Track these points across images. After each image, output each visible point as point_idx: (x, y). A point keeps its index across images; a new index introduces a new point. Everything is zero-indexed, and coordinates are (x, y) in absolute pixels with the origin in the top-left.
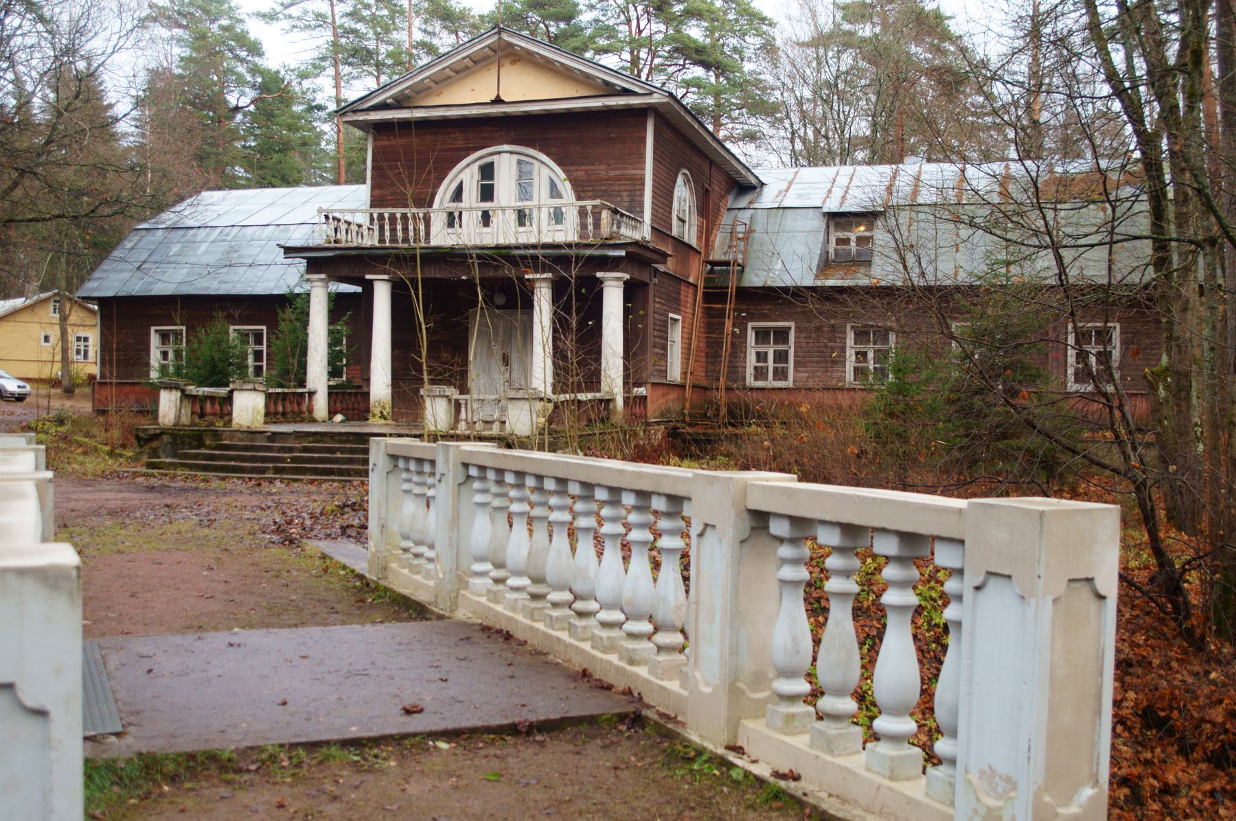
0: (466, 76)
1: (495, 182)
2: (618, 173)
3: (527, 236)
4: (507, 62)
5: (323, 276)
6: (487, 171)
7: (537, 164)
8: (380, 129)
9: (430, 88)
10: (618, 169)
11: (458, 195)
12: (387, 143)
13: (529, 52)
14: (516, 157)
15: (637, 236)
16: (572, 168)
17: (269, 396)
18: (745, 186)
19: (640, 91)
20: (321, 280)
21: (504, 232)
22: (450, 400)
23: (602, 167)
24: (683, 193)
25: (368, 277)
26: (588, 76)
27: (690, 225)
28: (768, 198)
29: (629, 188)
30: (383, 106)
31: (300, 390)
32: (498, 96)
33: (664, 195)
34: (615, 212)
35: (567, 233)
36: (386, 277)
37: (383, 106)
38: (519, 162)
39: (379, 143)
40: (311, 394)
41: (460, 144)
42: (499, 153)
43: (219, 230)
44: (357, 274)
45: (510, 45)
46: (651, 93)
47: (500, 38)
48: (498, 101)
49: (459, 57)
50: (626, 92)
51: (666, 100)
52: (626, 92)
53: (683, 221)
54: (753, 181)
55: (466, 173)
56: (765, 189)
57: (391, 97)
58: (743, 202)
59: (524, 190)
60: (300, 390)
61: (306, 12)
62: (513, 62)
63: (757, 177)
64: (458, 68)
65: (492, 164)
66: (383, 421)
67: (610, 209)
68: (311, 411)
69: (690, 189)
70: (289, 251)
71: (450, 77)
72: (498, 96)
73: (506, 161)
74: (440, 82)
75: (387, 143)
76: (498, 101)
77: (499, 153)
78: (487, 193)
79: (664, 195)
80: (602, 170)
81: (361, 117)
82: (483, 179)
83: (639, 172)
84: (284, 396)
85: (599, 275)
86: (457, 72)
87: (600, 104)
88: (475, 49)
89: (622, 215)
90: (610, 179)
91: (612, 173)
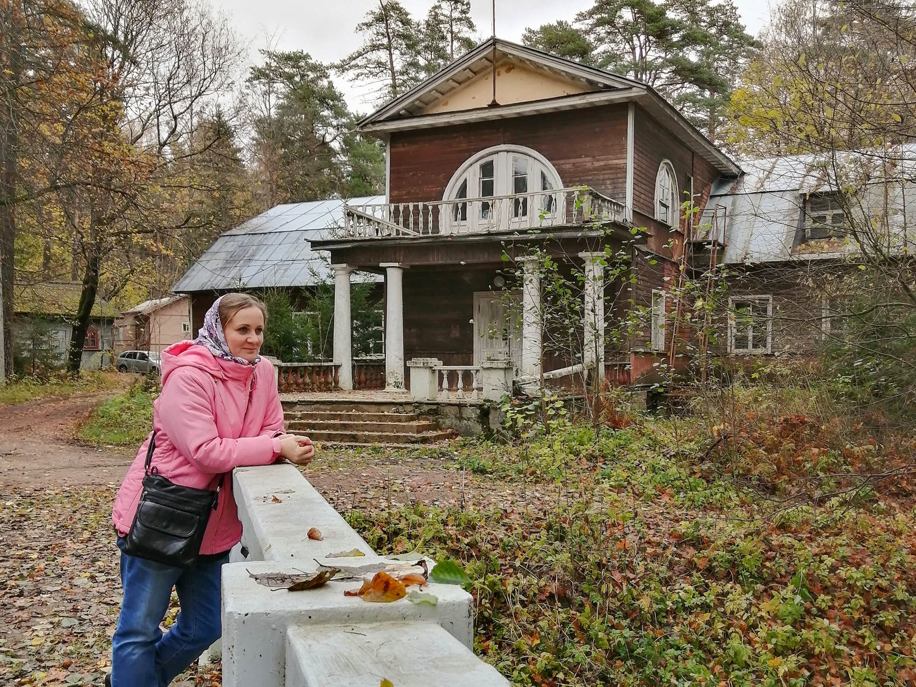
0: (469, 86)
1: (494, 179)
2: (602, 163)
3: (523, 223)
4: (503, 71)
5: (344, 265)
6: (488, 169)
7: (531, 160)
8: (395, 138)
9: (437, 98)
10: (604, 160)
11: (463, 192)
12: (402, 149)
13: (521, 60)
14: (511, 155)
15: (619, 219)
16: (561, 162)
17: (280, 368)
18: (727, 178)
19: (621, 87)
20: (343, 269)
21: (503, 219)
22: (434, 371)
23: (588, 159)
24: (665, 183)
25: (382, 265)
26: (574, 77)
27: (673, 211)
28: (750, 183)
29: (612, 176)
30: (397, 117)
31: (330, 364)
32: (494, 101)
33: (646, 182)
34: (596, 197)
35: (558, 218)
36: (397, 264)
37: (397, 117)
38: (515, 160)
39: (394, 150)
40: (337, 367)
41: (464, 146)
42: (497, 152)
43: (283, 235)
44: (372, 263)
45: (505, 55)
46: (631, 88)
47: (495, 48)
48: (494, 105)
49: (460, 69)
50: (608, 88)
51: (645, 92)
52: (608, 88)
53: (667, 207)
54: (735, 170)
55: (469, 173)
56: (746, 178)
57: (403, 108)
58: (726, 189)
59: (520, 184)
60: (330, 364)
61: (369, 61)
62: (508, 71)
63: (738, 167)
64: (460, 80)
65: (491, 163)
66: (397, 390)
67: (591, 194)
68: (337, 382)
69: (673, 177)
70: (315, 245)
71: (454, 88)
72: (494, 101)
73: (506, 160)
74: (445, 93)
75: (402, 149)
76: (494, 105)
77: (497, 152)
78: (488, 188)
79: (646, 182)
80: (587, 162)
81: (378, 128)
82: (484, 176)
83: (621, 161)
84: (295, 370)
85: (580, 255)
86: (460, 83)
87: (584, 101)
88: (473, 60)
89: (604, 200)
90: (595, 169)
91: (597, 164)
